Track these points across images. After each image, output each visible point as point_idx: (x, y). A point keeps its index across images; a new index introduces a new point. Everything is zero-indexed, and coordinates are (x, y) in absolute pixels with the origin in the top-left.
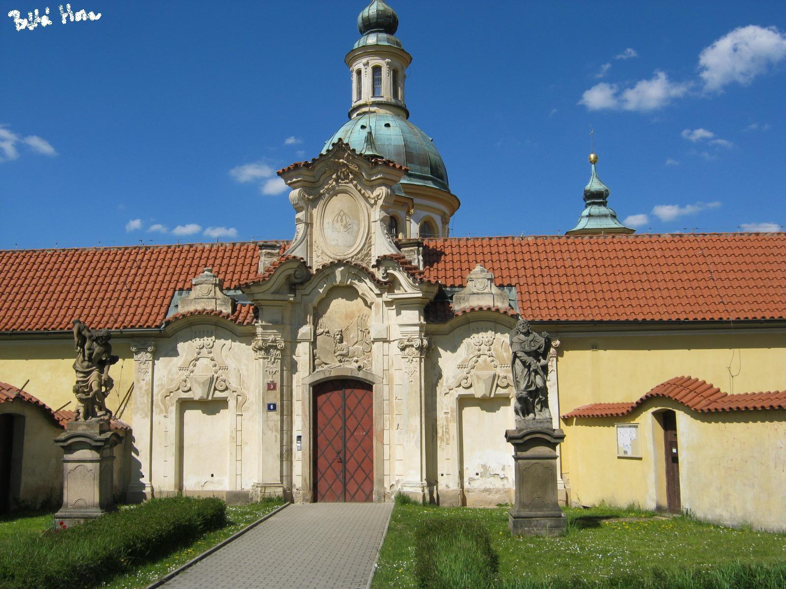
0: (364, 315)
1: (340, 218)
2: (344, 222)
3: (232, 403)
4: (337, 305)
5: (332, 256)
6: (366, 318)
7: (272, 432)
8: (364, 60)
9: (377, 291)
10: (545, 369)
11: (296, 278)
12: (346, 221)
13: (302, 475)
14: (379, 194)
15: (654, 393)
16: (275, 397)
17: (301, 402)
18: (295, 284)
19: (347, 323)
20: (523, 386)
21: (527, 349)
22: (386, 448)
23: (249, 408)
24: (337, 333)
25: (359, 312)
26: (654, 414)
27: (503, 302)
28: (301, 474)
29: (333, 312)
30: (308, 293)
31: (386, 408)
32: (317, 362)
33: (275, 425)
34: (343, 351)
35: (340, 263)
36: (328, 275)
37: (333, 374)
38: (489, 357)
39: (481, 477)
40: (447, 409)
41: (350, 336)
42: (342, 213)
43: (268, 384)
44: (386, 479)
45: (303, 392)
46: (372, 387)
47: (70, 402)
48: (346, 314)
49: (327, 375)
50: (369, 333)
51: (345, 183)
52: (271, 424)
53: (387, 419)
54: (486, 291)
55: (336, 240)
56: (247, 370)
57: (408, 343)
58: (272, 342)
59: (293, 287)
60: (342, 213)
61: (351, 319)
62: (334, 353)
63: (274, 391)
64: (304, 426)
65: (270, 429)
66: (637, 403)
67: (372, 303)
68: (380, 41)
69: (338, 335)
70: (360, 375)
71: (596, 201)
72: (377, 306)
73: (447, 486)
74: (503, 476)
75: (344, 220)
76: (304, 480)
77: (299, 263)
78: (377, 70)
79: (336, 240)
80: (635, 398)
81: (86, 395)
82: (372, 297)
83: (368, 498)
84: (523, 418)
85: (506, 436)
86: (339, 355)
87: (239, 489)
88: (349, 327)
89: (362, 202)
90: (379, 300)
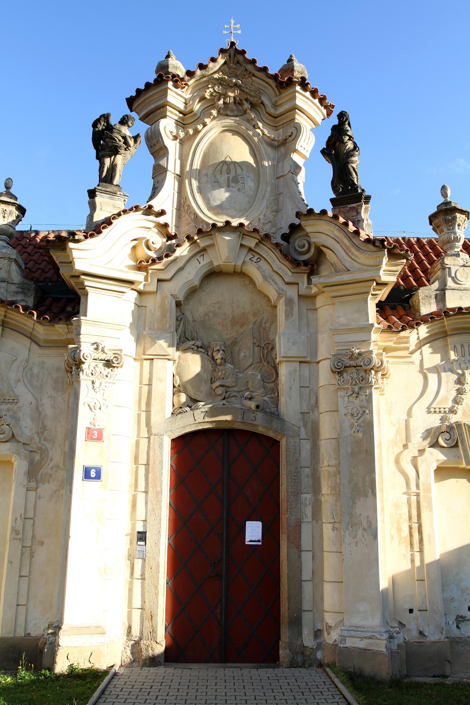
0: (264, 321)
2: (232, 174)
4: (219, 302)
6: (268, 325)
12: (236, 172)
14: (290, 134)
19: (235, 333)
22: (306, 558)
23: (51, 475)
24: (218, 348)
25: (254, 315)
29: (211, 314)
31: (306, 482)
34: (227, 379)
41: (239, 354)
43: (89, 429)
44: (306, 618)
46: (276, 444)
48: (234, 317)
50: (273, 348)
53: (308, 503)
56: (53, 407)
61: (242, 326)
62: (212, 382)
73: (421, 633)
75: (233, 171)
82: (279, 288)
86: (221, 386)
87: (21, 633)
88: (238, 340)
90: (292, 292)
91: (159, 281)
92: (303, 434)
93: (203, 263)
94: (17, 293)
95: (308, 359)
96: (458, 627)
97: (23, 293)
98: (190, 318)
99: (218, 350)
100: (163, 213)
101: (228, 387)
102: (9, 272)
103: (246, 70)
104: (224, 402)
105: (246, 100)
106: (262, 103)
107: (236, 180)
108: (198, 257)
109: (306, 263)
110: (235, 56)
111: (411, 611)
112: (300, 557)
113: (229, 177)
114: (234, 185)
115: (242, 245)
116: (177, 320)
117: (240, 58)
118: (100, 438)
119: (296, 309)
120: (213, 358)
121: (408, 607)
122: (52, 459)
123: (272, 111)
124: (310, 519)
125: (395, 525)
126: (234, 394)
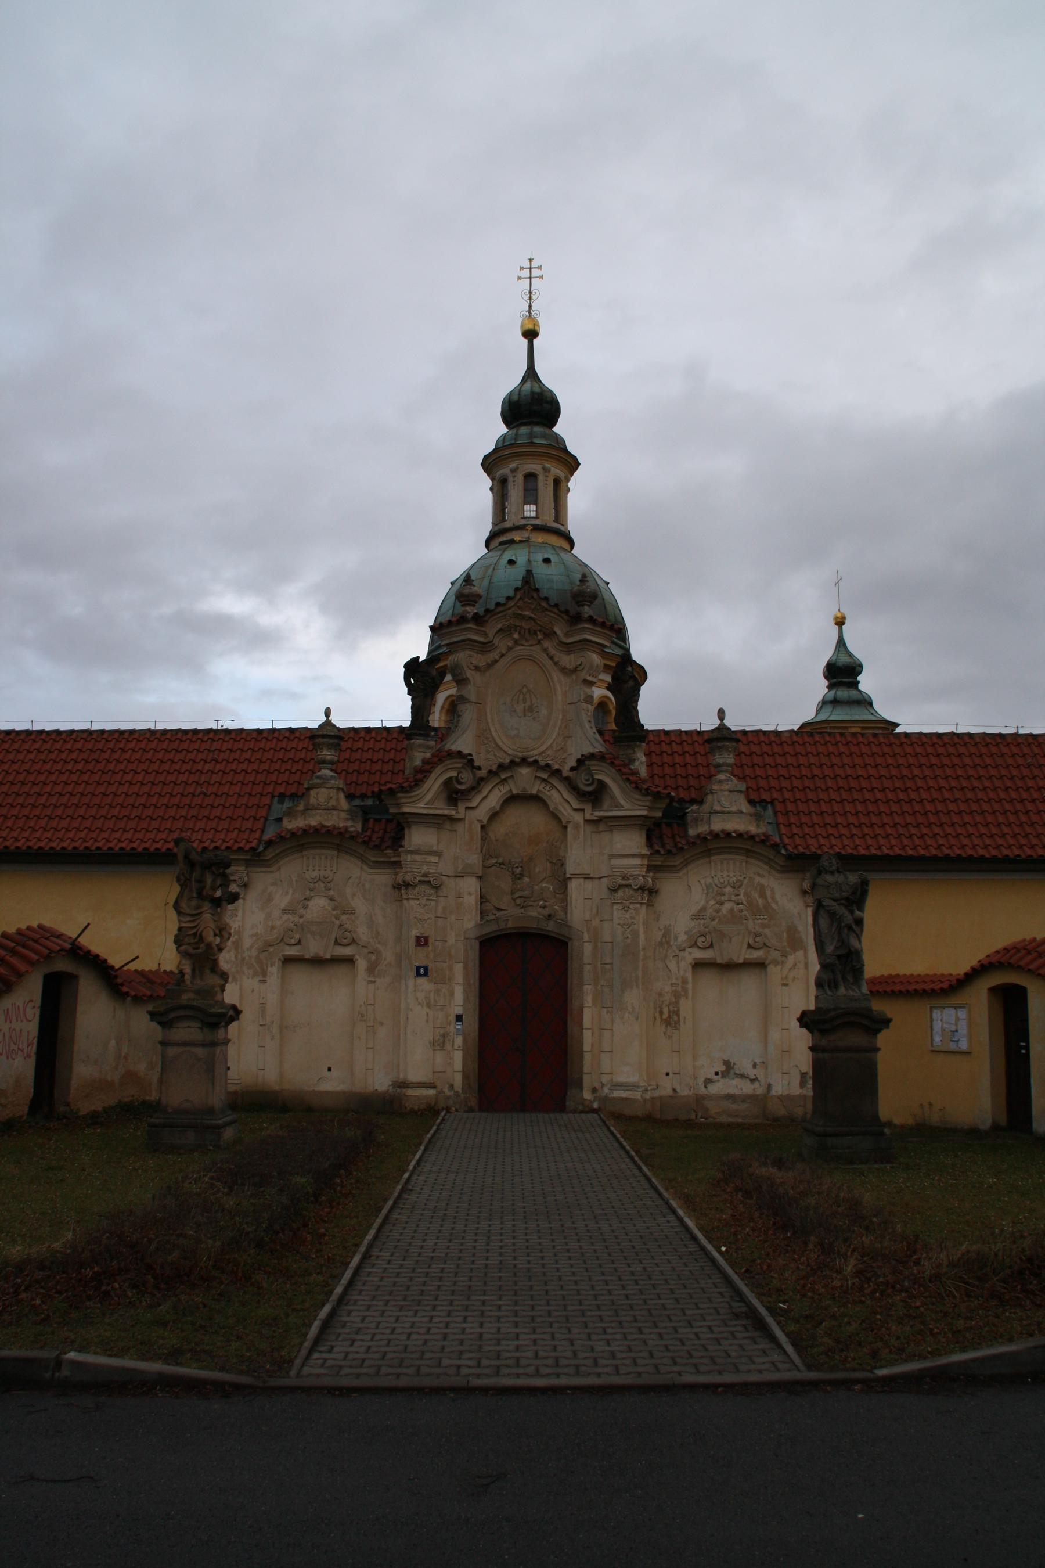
1: (521, 697)
2: (528, 704)
3: (362, 964)
5: (510, 752)
7: (422, 1006)
8: (512, 465)
9: (576, 805)
10: (859, 922)
11: (460, 783)
13: (463, 1071)
15: (994, 960)
16: (427, 956)
17: (461, 964)
18: (457, 792)
20: (830, 949)
21: (837, 895)
26: (992, 990)
27: (758, 826)
28: (461, 1069)
30: (474, 804)
32: (488, 906)
33: (426, 997)
35: (524, 762)
36: (505, 780)
37: (510, 925)
38: (738, 904)
39: (722, 1077)
40: (677, 979)
42: (525, 690)
44: (587, 1080)
45: (466, 950)
46: (566, 944)
47: (137, 957)
49: (502, 926)
51: (531, 645)
52: (421, 996)
54: (734, 809)
55: (516, 729)
57: (623, 882)
58: (425, 875)
59: (454, 796)
60: (525, 690)
62: (512, 893)
63: (425, 948)
64: (466, 999)
65: (419, 1004)
66: (966, 974)
67: (569, 822)
68: (536, 437)
69: (517, 867)
70: (550, 927)
71: (844, 680)
72: (577, 826)
73: (674, 1090)
74: (754, 1077)
76: (466, 1076)
77: (465, 761)
78: (530, 477)
79: (516, 729)
80: (961, 967)
81: (194, 948)
83: (562, 1108)
84: (829, 993)
85: (800, 1020)
86: (520, 897)
89: (556, 676)
91: (467, 808)
92: (586, 937)
93: (503, 791)
94: (347, 819)
95: (591, 876)
96: (705, 1087)
97: (352, 819)
98: (493, 837)
99: (517, 867)
100: (470, 755)
101: (525, 897)
102: (338, 800)
103: (540, 605)
104: (522, 910)
105: (540, 631)
106: (555, 633)
107: (531, 709)
108: (499, 786)
109: (590, 793)
110: (529, 592)
111: (667, 1074)
112: (582, 1033)
113: (525, 707)
114: (530, 714)
115: (536, 777)
116: (482, 839)
117: (535, 595)
118: (426, 944)
119: (582, 832)
120: (513, 873)
121: (666, 1071)
122: (385, 959)
123: (564, 640)
124: (591, 1005)
125: (658, 1010)
126: (531, 903)
